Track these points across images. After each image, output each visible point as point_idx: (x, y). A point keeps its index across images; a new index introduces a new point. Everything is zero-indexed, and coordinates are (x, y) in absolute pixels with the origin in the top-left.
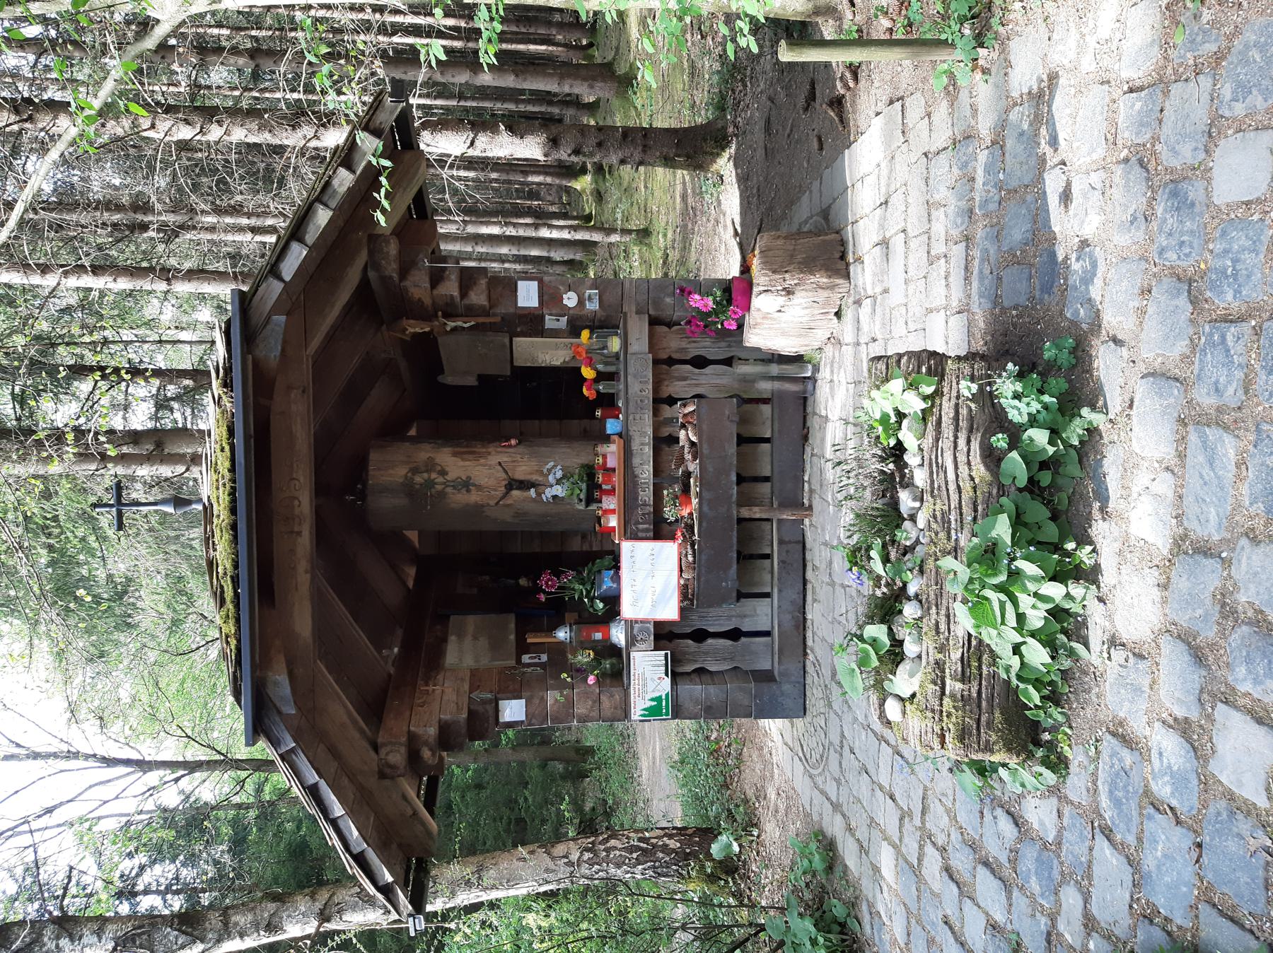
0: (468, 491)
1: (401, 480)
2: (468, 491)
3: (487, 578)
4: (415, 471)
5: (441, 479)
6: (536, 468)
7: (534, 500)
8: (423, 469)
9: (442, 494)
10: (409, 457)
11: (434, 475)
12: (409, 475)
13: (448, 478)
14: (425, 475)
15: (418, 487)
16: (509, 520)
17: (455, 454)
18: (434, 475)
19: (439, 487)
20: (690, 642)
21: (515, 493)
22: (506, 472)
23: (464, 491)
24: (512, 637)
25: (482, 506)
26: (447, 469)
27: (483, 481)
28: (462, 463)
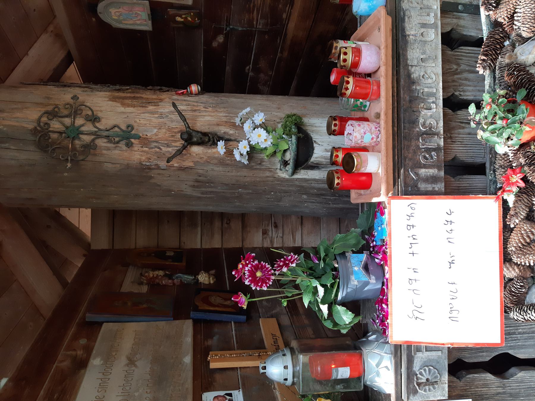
0: (129, 145)
1: (31, 126)
2: (129, 145)
3: (161, 273)
4: (53, 114)
5: (89, 127)
6: (224, 119)
7: (221, 162)
8: (66, 112)
9: (89, 148)
10: (48, 98)
11: (79, 121)
12: (44, 119)
13: (101, 126)
14: (68, 121)
15: (54, 136)
16: (189, 191)
17: (114, 99)
18: (79, 121)
19: (87, 139)
20: (489, 376)
21: (195, 149)
22: (184, 120)
23: (122, 145)
24: (188, 359)
25: (149, 168)
26: (100, 115)
27: (151, 133)
28: (122, 109)
